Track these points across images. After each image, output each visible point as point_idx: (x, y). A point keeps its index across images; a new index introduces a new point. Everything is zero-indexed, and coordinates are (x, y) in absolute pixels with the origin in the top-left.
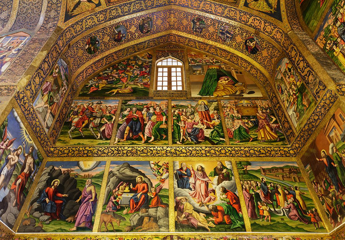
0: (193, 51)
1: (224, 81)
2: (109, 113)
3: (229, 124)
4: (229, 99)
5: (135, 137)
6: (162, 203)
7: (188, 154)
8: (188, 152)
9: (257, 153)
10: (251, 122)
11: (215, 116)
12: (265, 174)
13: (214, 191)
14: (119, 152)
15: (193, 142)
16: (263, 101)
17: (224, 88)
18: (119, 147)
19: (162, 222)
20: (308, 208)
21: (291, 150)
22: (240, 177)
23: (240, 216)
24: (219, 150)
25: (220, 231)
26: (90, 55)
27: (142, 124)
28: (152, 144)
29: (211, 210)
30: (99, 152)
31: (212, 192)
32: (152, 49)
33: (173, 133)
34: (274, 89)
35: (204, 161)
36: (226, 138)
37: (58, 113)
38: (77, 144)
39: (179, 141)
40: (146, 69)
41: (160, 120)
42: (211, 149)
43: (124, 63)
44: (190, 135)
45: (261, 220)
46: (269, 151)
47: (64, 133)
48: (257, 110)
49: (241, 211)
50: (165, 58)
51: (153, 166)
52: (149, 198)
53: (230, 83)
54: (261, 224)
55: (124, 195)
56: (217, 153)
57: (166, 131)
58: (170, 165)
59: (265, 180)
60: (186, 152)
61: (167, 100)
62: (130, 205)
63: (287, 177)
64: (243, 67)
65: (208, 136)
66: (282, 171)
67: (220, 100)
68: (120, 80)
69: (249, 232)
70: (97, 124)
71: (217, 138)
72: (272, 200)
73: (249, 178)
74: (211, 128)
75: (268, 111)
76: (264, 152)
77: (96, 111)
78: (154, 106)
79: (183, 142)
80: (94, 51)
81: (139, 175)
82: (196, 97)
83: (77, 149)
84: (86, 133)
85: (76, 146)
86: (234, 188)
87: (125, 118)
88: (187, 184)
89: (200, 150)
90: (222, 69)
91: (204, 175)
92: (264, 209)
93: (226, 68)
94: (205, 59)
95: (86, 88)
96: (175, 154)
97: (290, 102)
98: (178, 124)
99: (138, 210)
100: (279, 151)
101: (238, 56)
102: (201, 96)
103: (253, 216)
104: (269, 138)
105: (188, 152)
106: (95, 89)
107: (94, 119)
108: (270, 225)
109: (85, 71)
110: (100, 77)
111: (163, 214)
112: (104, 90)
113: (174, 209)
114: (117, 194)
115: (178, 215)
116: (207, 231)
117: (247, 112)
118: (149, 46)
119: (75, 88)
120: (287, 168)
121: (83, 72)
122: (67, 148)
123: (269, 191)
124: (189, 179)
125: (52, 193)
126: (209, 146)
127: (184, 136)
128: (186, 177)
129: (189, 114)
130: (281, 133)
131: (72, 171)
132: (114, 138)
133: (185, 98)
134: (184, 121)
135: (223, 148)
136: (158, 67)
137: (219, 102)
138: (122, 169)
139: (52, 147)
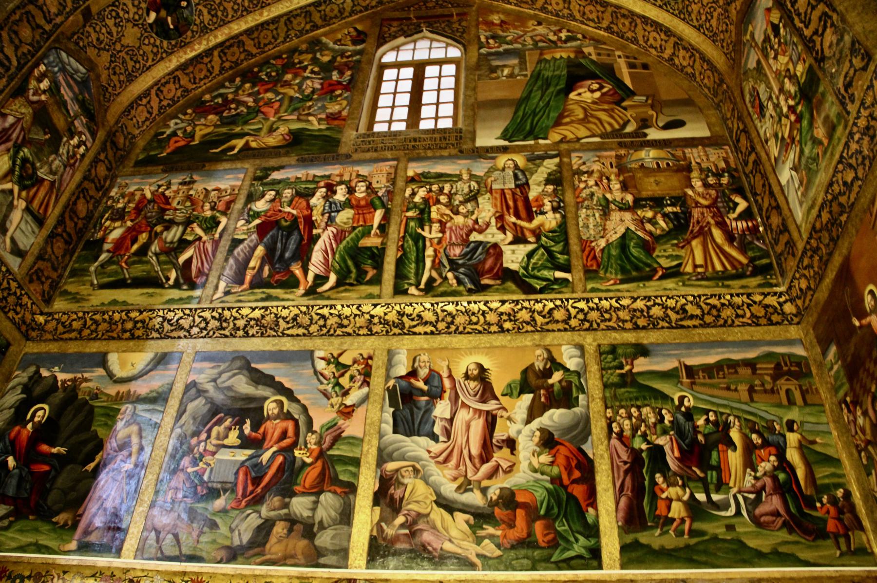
0: (498, 12)
1: (588, 94)
2: (213, 209)
3: (591, 226)
4: (598, 148)
5: (277, 277)
6: (335, 480)
7: (441, 326)
8: (443, 320)
9: (673, 316)
10: (665, 216)
11: (546, 201)
12: (693, 383)
13: (511, 444)
14: (224, 325)
15: (461, 288)
16: (710, 151)
17: (586, 116)
18: (223, 309)
19: (328, 539)
20: (826, 489)
21: (789, 304)
22: (608, 395)
23: (590, 520)
24: (547, 309)
25: (514, 569)
26: (165, 43)
27: (306, 237)
28: (329, 298)
29: (492, 504)
30: (165, 324)
31: (504, 445)
32: (368, 17)
33: (400, 263)
34: (740, 106)
35: (490, 350)
36: (574, 271)
37: (57, 211)
38: (110, 303)
39: (417, 286)
40: (341, 73)
41: (365, 221)
42: (519, 307)
43: (279, 62)
44: (454, 265)
45: (658, 531)
46: (714, 307)
48: (689, 179)
49: (593, 504)
50: (409, 39)
51: (321, 365)
52: (298, 464)
53: (607, 98)
54: (656, 545)
55: (224, 455)
56: (539, 320)
57: (377, 256)
59: (690, 402)
60: (433, 319)
61: (393, 160)
62: (236, 485)
63: (765, 391)
64: (651, 46)
65: (514, 267)
66: (749, 371)
67: (568, 153)
68: (259, 111)
69: (611, 570)
70: (172, 242)
71: (546, 273)
72: (705, 466)
73: (637, 399)
74: (525, 242)
75: (725, 180)
76: (698, 312)
77: (174, 204)
78: (350, 181)
79: (429, 289)
80: (176, 28)
81: (274, 395)
82: (492, 148)
83: (106, 317)
84: (138, 270)
85: (105, 308)
86: (582, 431)
87: (257, 221)
88: (426, 423)
89: (484, 312)
90: (585, 57)
91: (487, 392)
92: (674, 497)
93: (599, 54)
94: (536, 32)
95: (159, 141)
96: (399, 327)
97: (783, 137)
98: (419, 231)
99: (257, 501)
100: (749, 305)
101: (632, 13)
102: (506, 143)
103: (633, 519)
104: (719, 267)
105: (443, 320)
106: (182, 143)
107: (167, 229)
108: (687, 547)
109: (153, 92)
110: (201, 108)
111: (333, 514)
112: (209, 142)
113: (371, 498)
114: (201, 449)
115: (382, 519)
116: (472, 566)
117: (654, 187)
118: (358, 8)
119: (122, 140)
120: (768, 363)
121: (146, 93)
122: (80, 314)
123: (700, 437)
124: (434, 405)
125: (25, 444)
126: (515, 297)
127: (436, 270)
128: (426, 398)
129: (461, 199)
130: (760, 249)
131: (86, 380)
132: (215, 281)
133: (454, 151)
134: (440, 221)
135: (558, 303)
136: (383, 67)
137: (565, 160)
138: (225, 376)
139: (42, 314)
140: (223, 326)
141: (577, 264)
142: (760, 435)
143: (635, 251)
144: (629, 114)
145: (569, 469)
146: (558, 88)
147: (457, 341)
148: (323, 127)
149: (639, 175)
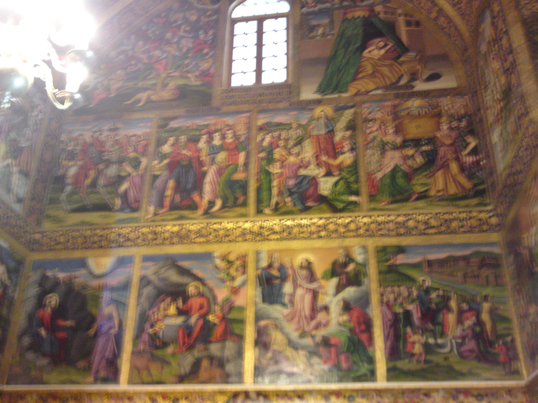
2: (135, 151)
4: (382, 99)
10: (422, 153)
13: (326, 308)
33: (259, 190)
35: (313, 250)
40: (206, 33)
44: (291, 193)
47: (54, 201)
48: (439, 124)
51: (218, 262)
57: (244, 186)
58: (251, 260)
59: (428, 283)
69: (381, 382)
72: (434, 321)
74: (334, 176)
75: (463, 124)
84: (93, 199)
87: (166, 161)
91: (312, 278)
93: (386, 13)
96: (260, 235)
99: (191, 347)
103: (393, 353)
107: (107, 166)
136: (235, 21)
138: (163, 270)
140: (156, 238)
141: (364, 190)
142: (468, 303)
143: (400, 181)
144: (404, 68)
145: (359, 323)
146: (356, 46)
147: (295, 244)
148: (198, 83)
149: (406, 121)
